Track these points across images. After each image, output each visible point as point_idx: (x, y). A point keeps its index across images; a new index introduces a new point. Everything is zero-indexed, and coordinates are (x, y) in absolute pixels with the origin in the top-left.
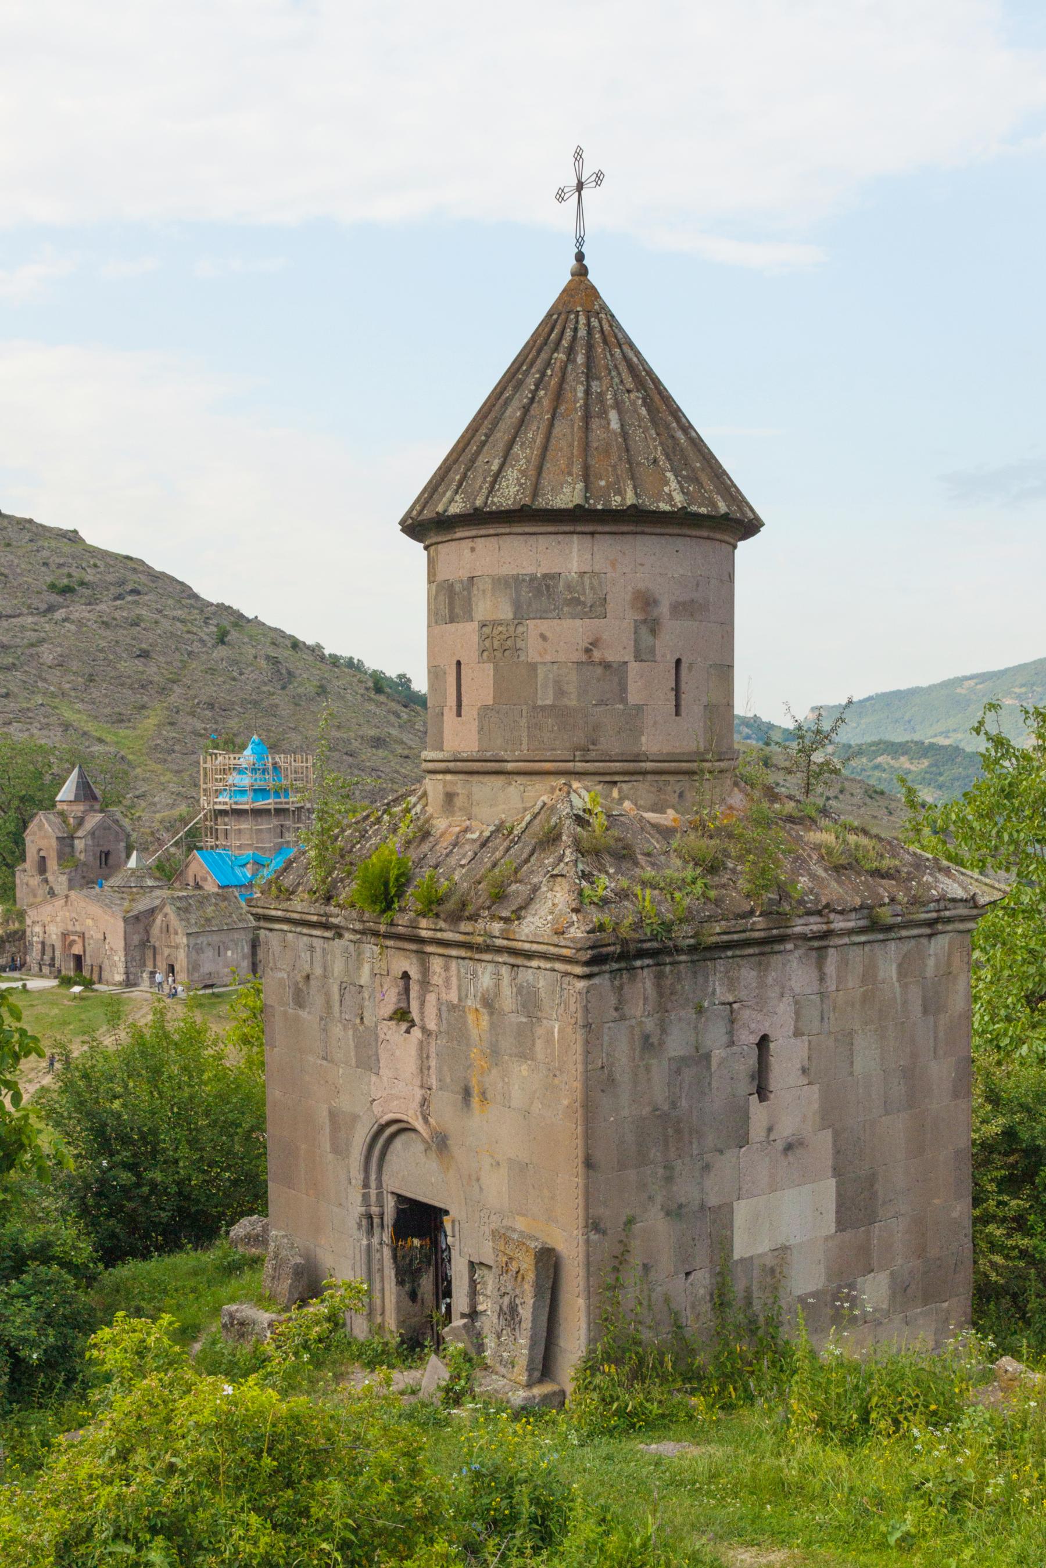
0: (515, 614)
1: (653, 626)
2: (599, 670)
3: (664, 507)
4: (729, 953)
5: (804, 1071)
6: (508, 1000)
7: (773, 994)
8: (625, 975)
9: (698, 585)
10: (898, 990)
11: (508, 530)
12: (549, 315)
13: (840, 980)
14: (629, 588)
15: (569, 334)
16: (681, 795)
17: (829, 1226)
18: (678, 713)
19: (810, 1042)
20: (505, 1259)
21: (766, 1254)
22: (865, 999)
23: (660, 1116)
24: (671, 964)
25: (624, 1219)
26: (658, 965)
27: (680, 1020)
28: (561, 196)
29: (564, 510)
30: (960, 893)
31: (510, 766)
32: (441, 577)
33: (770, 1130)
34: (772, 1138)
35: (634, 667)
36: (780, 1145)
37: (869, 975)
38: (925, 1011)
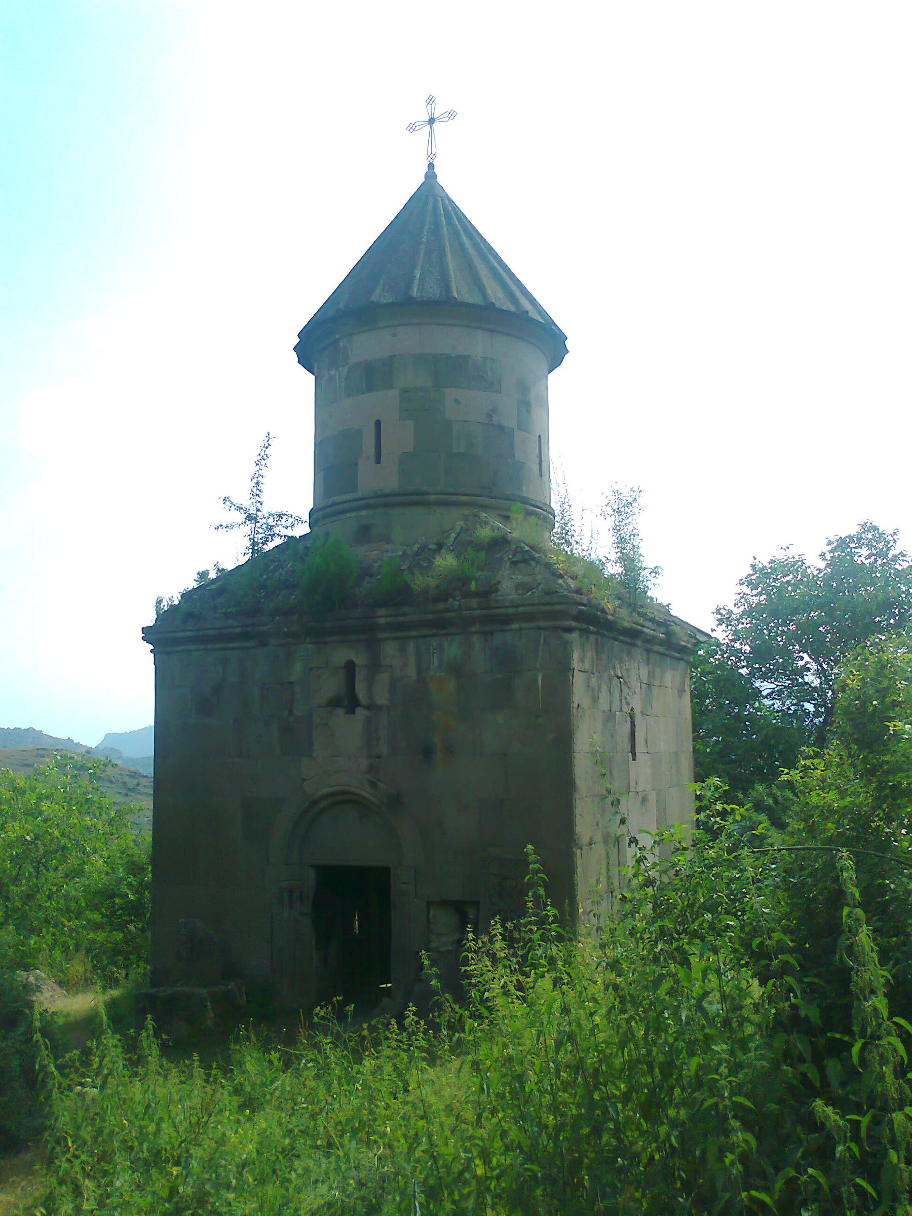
31: (432, 498)
35: (517, 432)
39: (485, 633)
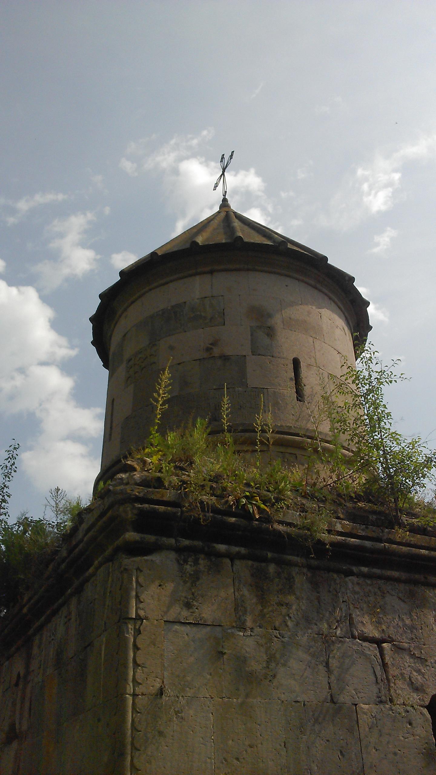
4: (365, 569)
8: (203, 562)
24: (280, 563)
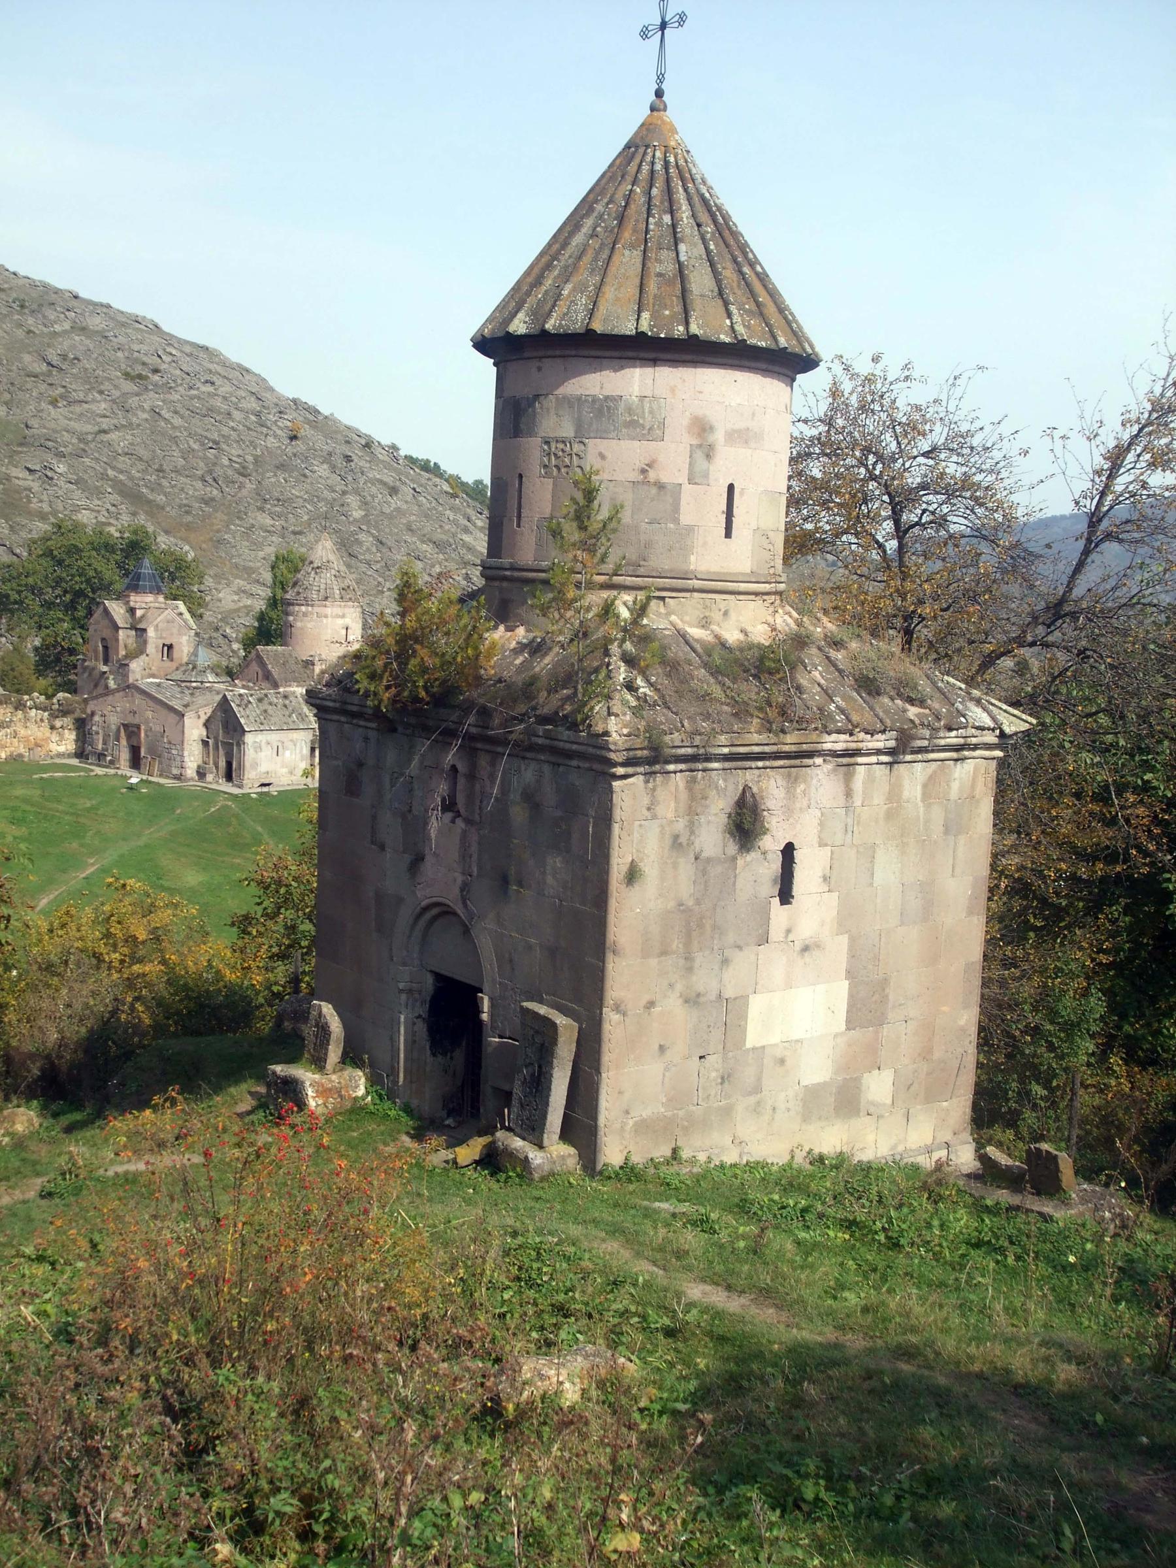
0: (576, 432)
1: (709, 453)
2: (654, 491)
3: (725, 338)
5: (825, 879)
6: (549, 796)
7: (801, 803)
9: (753, 414)
10: (922, 810)
11: (573, 353)
12: (628, 147)
13: (866, 796)
14: (687, 413)
15: (646, 168)
16: (726, 613)
17: (839, 1022)
18: (728, 534)
19: (832, 853)
20: (532, 1032)
21: (776, 1045)
22: (890, 815)
23: (684, 911)
24: (704, 770)
25: (643, 1002)
26: (692, 771)
27: (709, 822)
28: (645, 34)
29: (628, 336)
30: (988, 722)
32: (506, 394)
33: (788, 931)
34: (790, 939)
35: (687, 487)
36: (798, 946)
37: (894, 795)
38: (947, 831)
39: (554, 764)
